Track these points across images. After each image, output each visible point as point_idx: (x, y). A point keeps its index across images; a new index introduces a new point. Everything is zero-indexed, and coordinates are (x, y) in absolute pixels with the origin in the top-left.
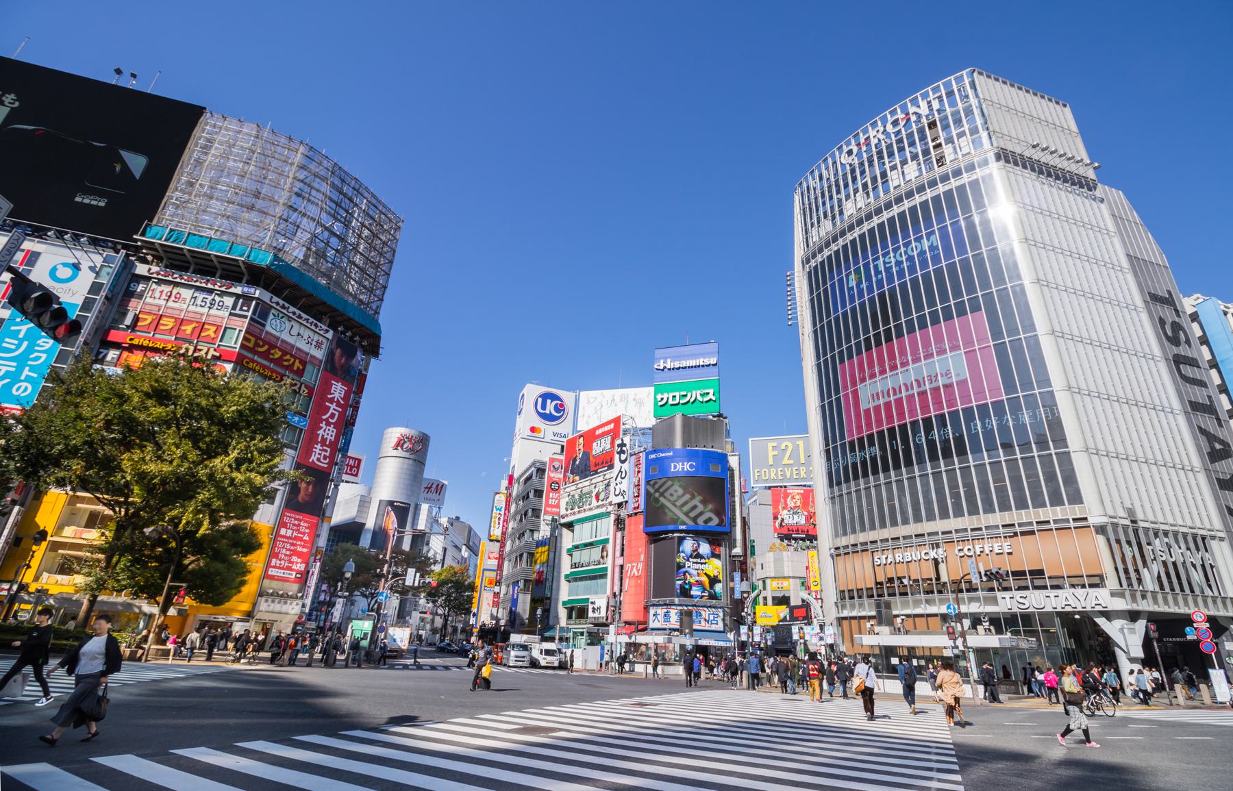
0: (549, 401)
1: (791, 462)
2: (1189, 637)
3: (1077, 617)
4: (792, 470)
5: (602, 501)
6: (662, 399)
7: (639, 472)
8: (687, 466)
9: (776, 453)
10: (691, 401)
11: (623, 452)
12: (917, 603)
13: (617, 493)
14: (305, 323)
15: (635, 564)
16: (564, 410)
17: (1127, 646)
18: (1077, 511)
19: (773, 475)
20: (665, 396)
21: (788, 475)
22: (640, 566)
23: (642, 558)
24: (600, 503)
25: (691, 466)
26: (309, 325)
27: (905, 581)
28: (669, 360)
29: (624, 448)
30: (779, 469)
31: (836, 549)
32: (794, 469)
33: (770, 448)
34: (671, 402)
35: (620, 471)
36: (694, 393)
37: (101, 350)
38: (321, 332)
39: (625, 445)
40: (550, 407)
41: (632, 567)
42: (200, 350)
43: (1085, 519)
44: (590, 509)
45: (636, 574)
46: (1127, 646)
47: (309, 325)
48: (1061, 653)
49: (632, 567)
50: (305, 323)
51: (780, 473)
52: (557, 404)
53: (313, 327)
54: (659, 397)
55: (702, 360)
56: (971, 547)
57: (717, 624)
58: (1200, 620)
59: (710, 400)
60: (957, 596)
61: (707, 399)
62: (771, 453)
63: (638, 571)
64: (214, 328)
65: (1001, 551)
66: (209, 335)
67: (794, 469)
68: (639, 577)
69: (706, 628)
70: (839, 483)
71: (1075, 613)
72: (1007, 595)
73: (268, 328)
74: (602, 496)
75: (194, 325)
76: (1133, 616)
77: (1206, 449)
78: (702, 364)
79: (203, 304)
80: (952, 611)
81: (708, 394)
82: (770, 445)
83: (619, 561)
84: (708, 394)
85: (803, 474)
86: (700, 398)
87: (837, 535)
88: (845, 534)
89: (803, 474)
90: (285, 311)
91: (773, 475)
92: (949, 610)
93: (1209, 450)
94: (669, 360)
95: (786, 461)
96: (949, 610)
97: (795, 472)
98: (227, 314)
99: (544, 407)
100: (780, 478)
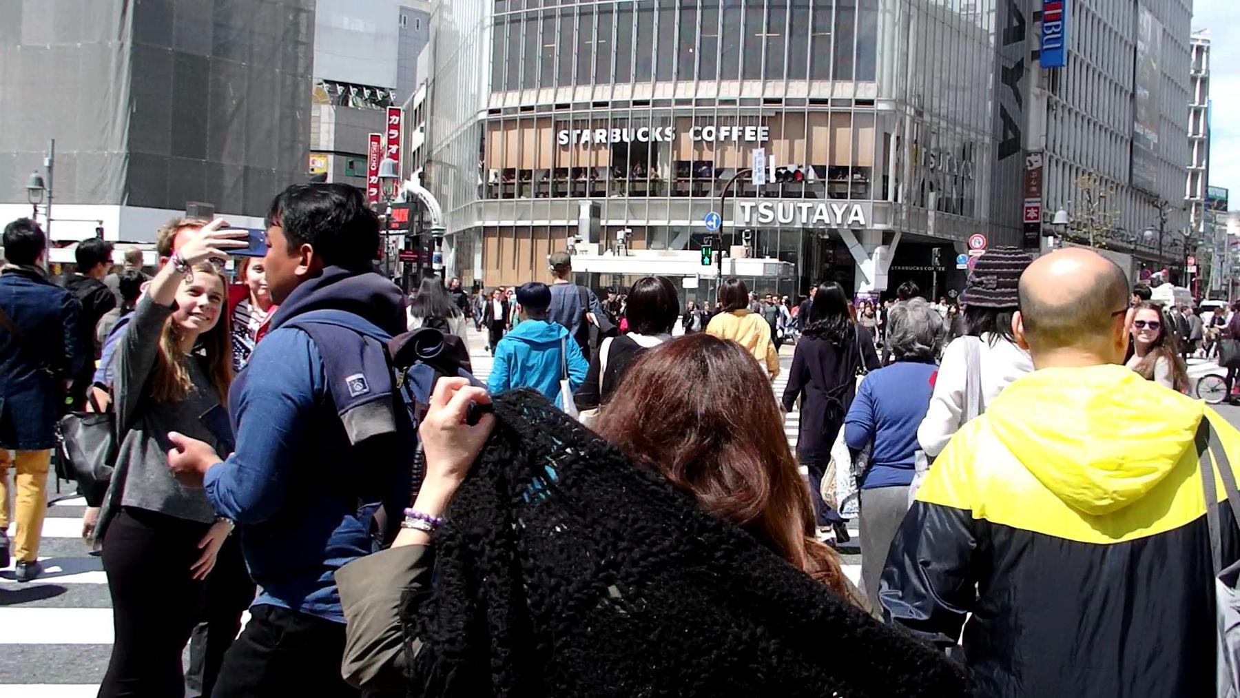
2: (959, 267)
3: (826, 237)
18: (867, 91)
31: (492, 112)
43: (871, 102)
48: (797, 282)
58: (977, 245)
60: (723, 200)
65: (754, 139)
71: (823, 232)
72: (748, 203)
80: (714, 224)
87: (495, 87)
88: (512, 86)
92: (710, 223)
93: (1006, 27)
96: (710, 223)
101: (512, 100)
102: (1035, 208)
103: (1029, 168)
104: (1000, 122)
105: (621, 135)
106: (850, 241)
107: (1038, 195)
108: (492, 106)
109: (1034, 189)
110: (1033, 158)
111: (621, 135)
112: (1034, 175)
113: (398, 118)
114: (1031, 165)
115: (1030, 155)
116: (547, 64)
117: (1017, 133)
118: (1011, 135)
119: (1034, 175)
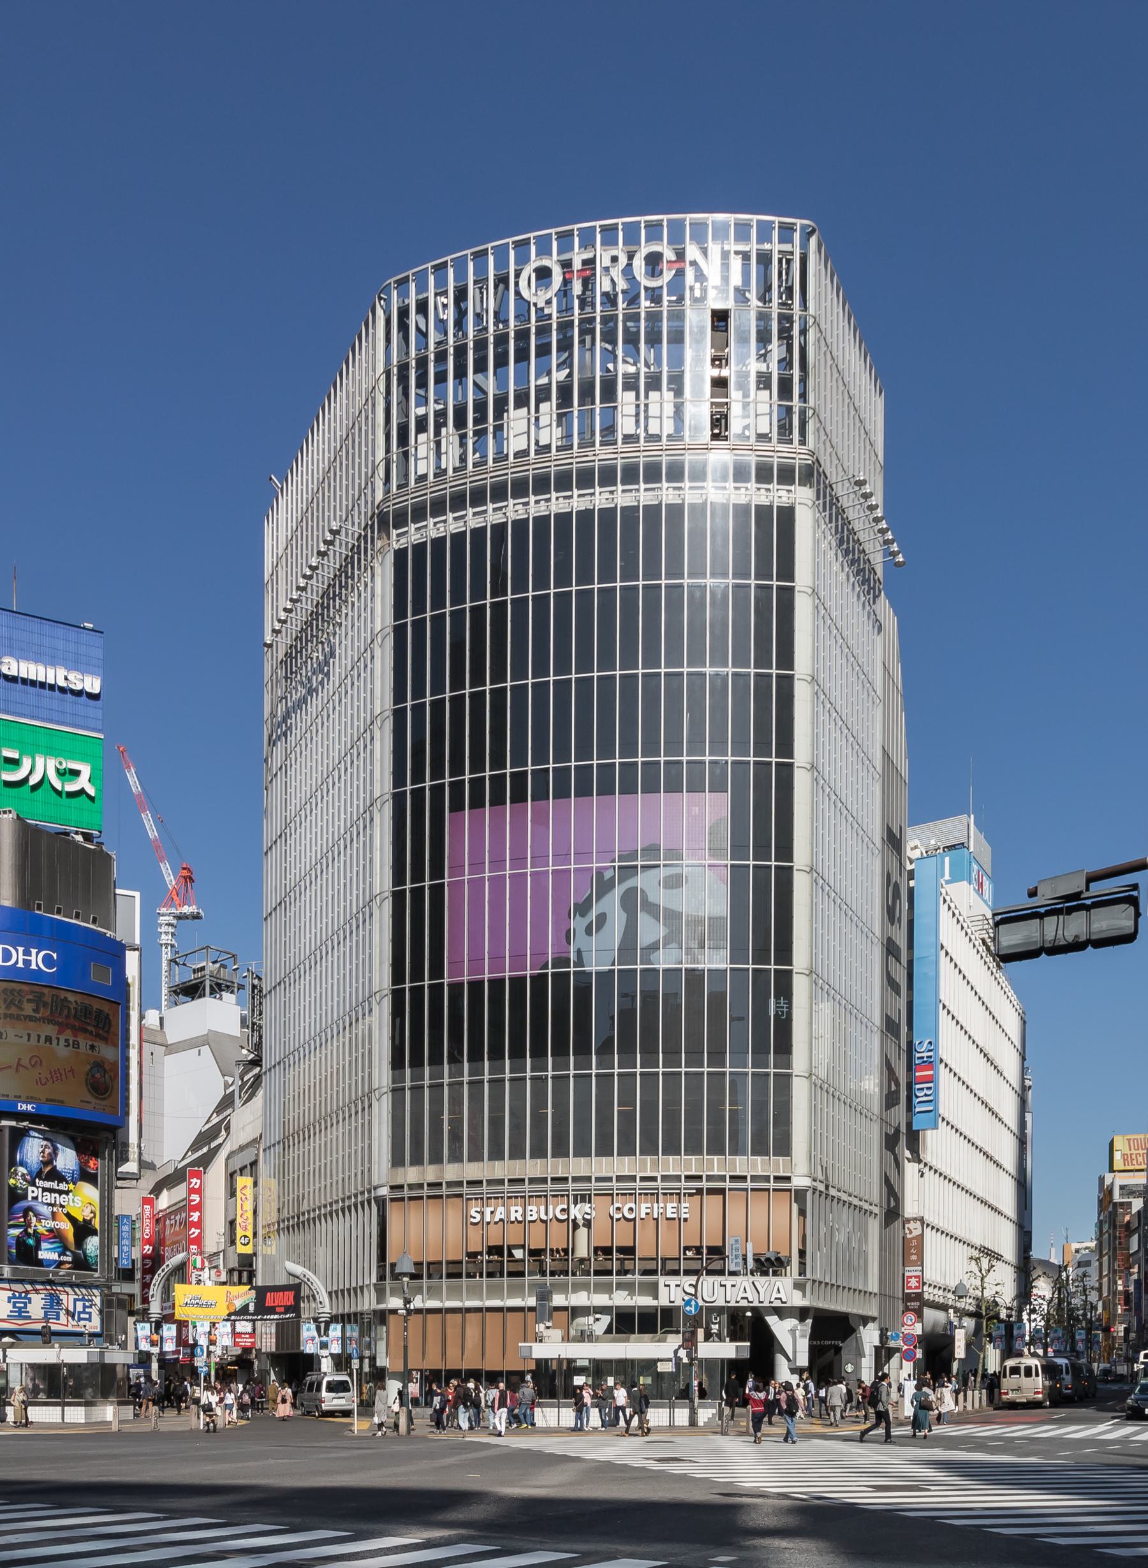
3: (749, 1314)
8: (37, 959)
10: (33, 780)
12: (577, 1288)
17: (795, 1352)
25: (47, 960)
27: (518, 1254)
31: (392, 1187)
36: (40, 761)
46: (795, 1352)
55: (61, 672)
56: (633, 1205)
57: (89, 1320)
59: (82, 792)
69: (70, 1328)
70: (417, 1062)
71: (745, 1309)
72: (672, 1281)
76: (802, 1313)
77: (885, 1092)
78: (62, 683)
81: (76, 773)
84: (76, 773)
87: (397, 1161)
101: (411, 1175)
102: (916, 1277)
103: (909, 1236)
104: (884, 1189)
105: (538, 1212)
106: (772, 1320)
107: (919, 1263)
109: (914, 1257)
110: (912, 1225)
111: (538, 1212)
112: (914, 1243)
113: (199, 1181)
114: (911, 1232)
115: (908, 1221)
116: (456, 1137)
117: (897, 1200)
118: (893, 1204)
119: (914, 1243)
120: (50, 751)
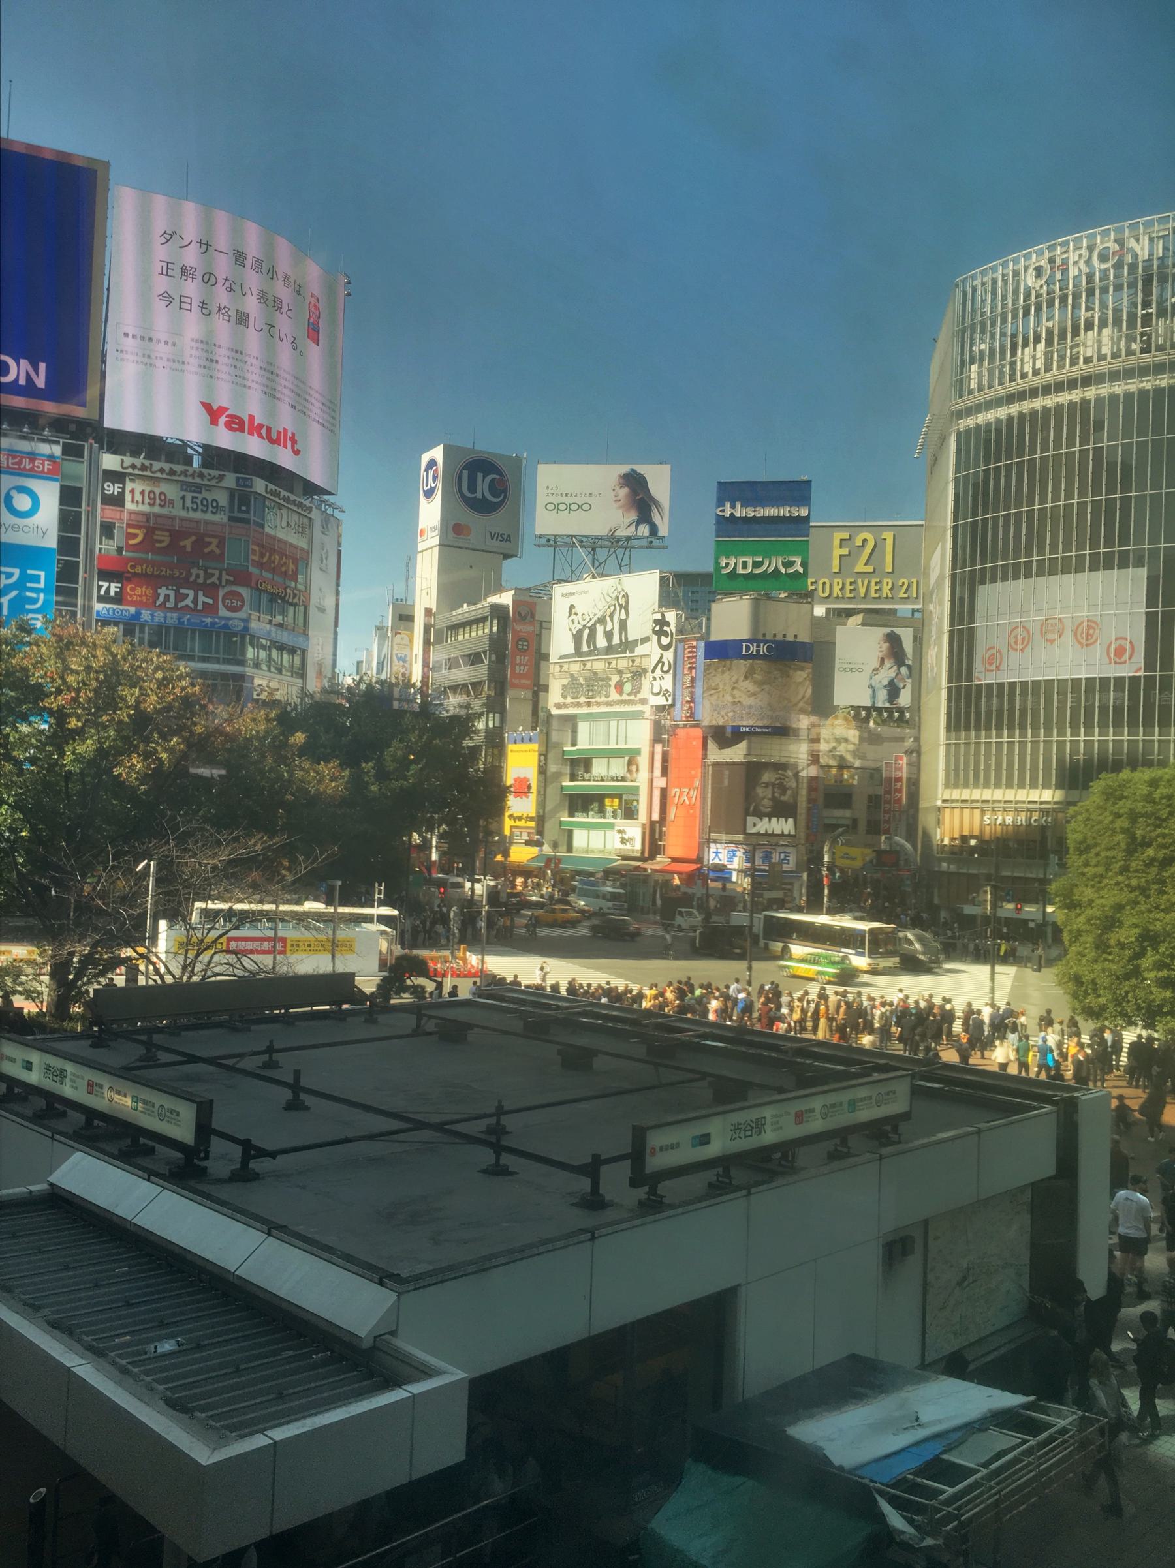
0: (480, 476)
1: (870, 569)
4: (869, 582)
5: (629, 694)
6: (727, 565)
7: (691, 669)
9: (845, 551)
10: (769, 571)
11: (666, 634)
13: (656, 690)
14: (292, 507)
15: (686, 790)
16: (505, 491)
19: (836, 590)
20: (732, 562)
21: (862, 591)
22: (693, 793)
23: (697, 783)
24: (625, 697)
26: (295, 509)
28: (738, 505)
29: (665, 628)
30: (848, 581)
31: (944, 801)
32: (874, 581)
33: (837, 542)
34: (740, 571)
35: (660, 661)
37: (100, 583)
38: (306, 514)
39: (668, 624)
40: (483, 486)
41: (681, 793)
42: (213, 575)
44: (608, 704)
45: (687, 802)
47: (295, 509)
49: (681, 793)
50: (292, 507)
51: (848, 587)
52: (493, 480)
53: (300, 510)
54: (723, 563)
61: (790, 571)
62: (837, 552)
63: (690, 799)
64: (215, 541)
66: (212, 551)
67: (874, 581)
68: (691, 806)
73: (267, 530)
74: (628, 687)
75: (193, 538)
79: (195, 507)
81: (792, 563)
82: (838, 536)
83: (660, 782)
84: (792, 563)
85: (886, 590)
86: (783, 571)
88: (956, 786)
89: (886, 590)
90: (277, 499)
91: (836, 590)
94: (738, 505)
95: (860, 567)
97: (873, 588)
98: (225, 519)
99: (472, 487)
100: (848, 595)
108: (945, 798)
120: (778, 553)
